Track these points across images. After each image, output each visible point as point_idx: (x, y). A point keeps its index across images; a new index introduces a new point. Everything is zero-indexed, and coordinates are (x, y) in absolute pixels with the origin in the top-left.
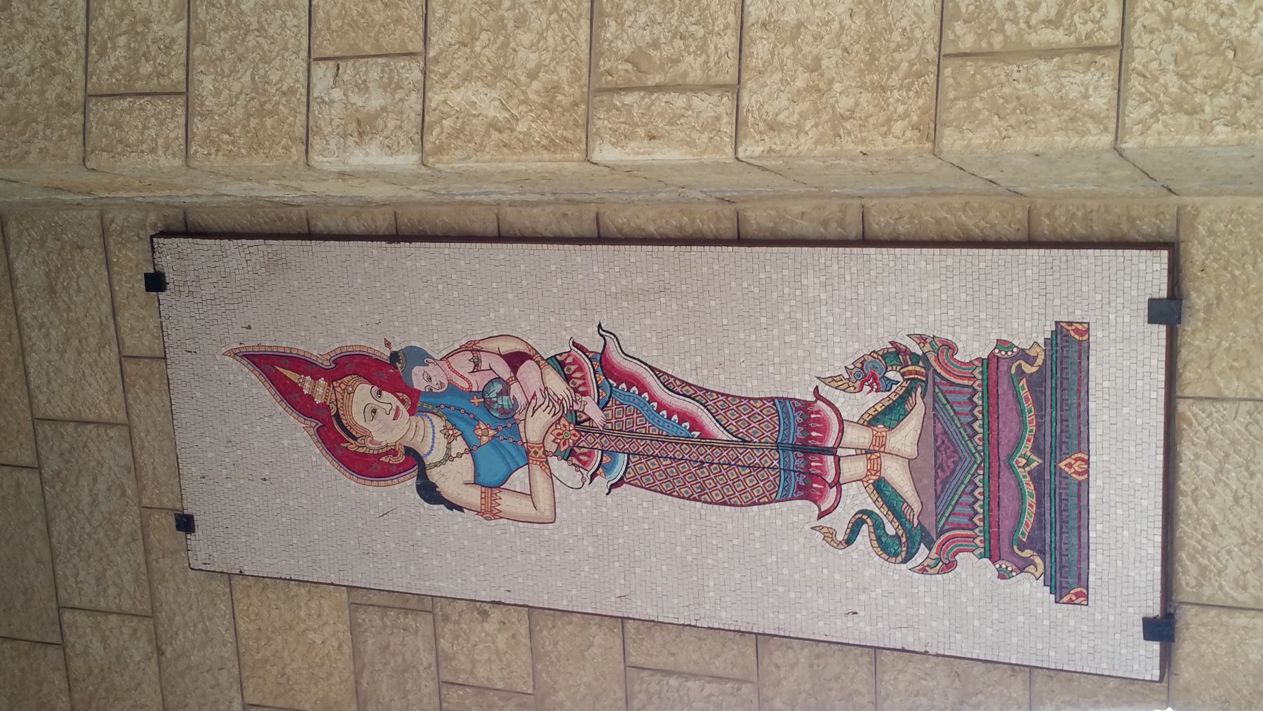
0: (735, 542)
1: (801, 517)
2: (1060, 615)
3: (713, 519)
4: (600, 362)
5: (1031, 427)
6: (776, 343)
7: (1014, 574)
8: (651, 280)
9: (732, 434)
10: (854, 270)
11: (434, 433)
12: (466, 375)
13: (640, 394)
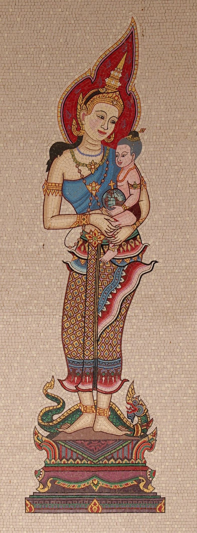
0: (42, 334)
1: (59, 370)
2: (19, 500)
3: (54, 322)
4: (137, 261)
5: (113, 486)
6: (151, 360)
7: (38, 478)
8: (182, 293)
9: (101, 334)
10: (189, 401)
11: (92, 156)
12: (126, 179)
13: (120, 283)
